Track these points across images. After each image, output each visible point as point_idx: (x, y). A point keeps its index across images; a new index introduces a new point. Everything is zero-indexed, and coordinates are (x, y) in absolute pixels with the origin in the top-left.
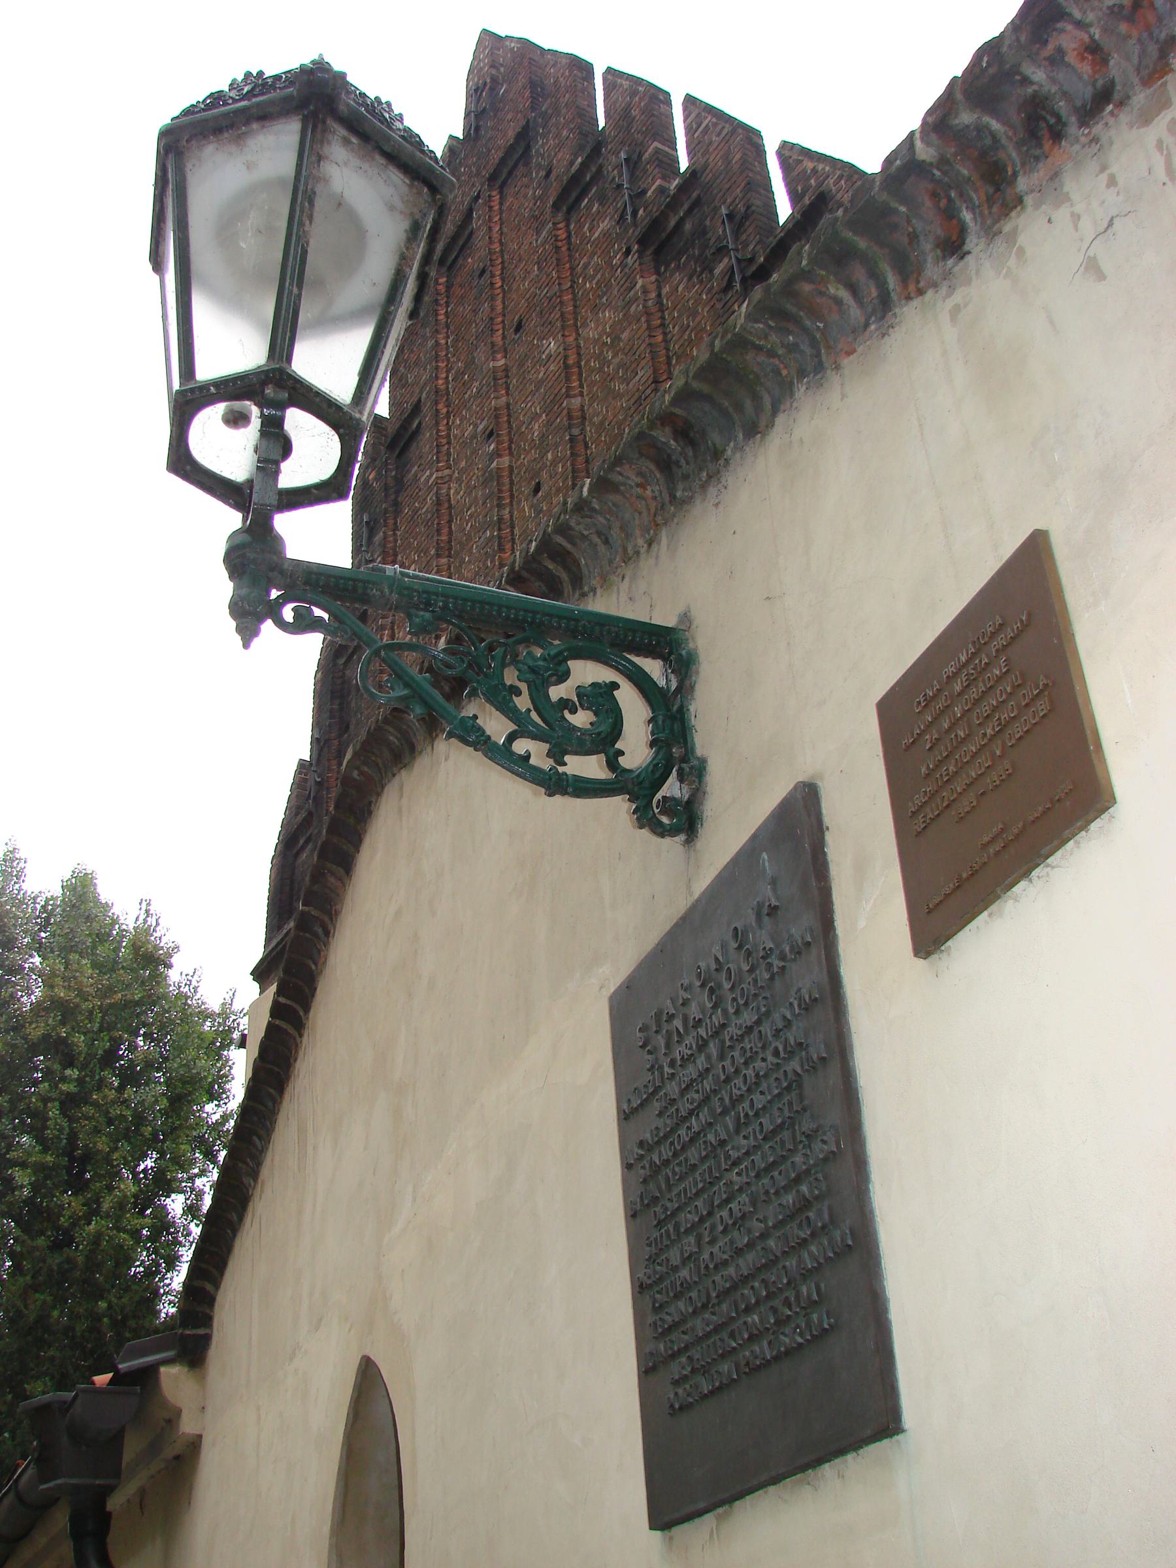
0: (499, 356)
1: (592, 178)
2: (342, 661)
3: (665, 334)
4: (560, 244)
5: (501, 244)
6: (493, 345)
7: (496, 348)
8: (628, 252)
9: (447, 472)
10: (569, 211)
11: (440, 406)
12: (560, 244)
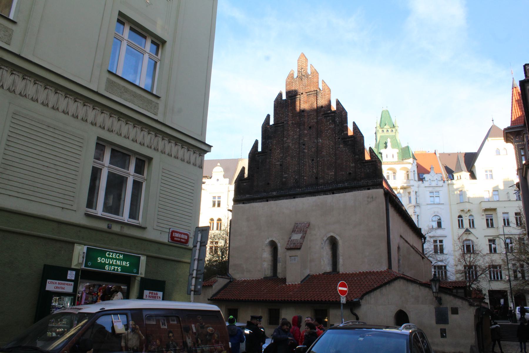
1: (331, 115)
2: (257, 155)
6: (305, 128)
8: (339, 138)
9: (290, 141)
10: (325, 117)
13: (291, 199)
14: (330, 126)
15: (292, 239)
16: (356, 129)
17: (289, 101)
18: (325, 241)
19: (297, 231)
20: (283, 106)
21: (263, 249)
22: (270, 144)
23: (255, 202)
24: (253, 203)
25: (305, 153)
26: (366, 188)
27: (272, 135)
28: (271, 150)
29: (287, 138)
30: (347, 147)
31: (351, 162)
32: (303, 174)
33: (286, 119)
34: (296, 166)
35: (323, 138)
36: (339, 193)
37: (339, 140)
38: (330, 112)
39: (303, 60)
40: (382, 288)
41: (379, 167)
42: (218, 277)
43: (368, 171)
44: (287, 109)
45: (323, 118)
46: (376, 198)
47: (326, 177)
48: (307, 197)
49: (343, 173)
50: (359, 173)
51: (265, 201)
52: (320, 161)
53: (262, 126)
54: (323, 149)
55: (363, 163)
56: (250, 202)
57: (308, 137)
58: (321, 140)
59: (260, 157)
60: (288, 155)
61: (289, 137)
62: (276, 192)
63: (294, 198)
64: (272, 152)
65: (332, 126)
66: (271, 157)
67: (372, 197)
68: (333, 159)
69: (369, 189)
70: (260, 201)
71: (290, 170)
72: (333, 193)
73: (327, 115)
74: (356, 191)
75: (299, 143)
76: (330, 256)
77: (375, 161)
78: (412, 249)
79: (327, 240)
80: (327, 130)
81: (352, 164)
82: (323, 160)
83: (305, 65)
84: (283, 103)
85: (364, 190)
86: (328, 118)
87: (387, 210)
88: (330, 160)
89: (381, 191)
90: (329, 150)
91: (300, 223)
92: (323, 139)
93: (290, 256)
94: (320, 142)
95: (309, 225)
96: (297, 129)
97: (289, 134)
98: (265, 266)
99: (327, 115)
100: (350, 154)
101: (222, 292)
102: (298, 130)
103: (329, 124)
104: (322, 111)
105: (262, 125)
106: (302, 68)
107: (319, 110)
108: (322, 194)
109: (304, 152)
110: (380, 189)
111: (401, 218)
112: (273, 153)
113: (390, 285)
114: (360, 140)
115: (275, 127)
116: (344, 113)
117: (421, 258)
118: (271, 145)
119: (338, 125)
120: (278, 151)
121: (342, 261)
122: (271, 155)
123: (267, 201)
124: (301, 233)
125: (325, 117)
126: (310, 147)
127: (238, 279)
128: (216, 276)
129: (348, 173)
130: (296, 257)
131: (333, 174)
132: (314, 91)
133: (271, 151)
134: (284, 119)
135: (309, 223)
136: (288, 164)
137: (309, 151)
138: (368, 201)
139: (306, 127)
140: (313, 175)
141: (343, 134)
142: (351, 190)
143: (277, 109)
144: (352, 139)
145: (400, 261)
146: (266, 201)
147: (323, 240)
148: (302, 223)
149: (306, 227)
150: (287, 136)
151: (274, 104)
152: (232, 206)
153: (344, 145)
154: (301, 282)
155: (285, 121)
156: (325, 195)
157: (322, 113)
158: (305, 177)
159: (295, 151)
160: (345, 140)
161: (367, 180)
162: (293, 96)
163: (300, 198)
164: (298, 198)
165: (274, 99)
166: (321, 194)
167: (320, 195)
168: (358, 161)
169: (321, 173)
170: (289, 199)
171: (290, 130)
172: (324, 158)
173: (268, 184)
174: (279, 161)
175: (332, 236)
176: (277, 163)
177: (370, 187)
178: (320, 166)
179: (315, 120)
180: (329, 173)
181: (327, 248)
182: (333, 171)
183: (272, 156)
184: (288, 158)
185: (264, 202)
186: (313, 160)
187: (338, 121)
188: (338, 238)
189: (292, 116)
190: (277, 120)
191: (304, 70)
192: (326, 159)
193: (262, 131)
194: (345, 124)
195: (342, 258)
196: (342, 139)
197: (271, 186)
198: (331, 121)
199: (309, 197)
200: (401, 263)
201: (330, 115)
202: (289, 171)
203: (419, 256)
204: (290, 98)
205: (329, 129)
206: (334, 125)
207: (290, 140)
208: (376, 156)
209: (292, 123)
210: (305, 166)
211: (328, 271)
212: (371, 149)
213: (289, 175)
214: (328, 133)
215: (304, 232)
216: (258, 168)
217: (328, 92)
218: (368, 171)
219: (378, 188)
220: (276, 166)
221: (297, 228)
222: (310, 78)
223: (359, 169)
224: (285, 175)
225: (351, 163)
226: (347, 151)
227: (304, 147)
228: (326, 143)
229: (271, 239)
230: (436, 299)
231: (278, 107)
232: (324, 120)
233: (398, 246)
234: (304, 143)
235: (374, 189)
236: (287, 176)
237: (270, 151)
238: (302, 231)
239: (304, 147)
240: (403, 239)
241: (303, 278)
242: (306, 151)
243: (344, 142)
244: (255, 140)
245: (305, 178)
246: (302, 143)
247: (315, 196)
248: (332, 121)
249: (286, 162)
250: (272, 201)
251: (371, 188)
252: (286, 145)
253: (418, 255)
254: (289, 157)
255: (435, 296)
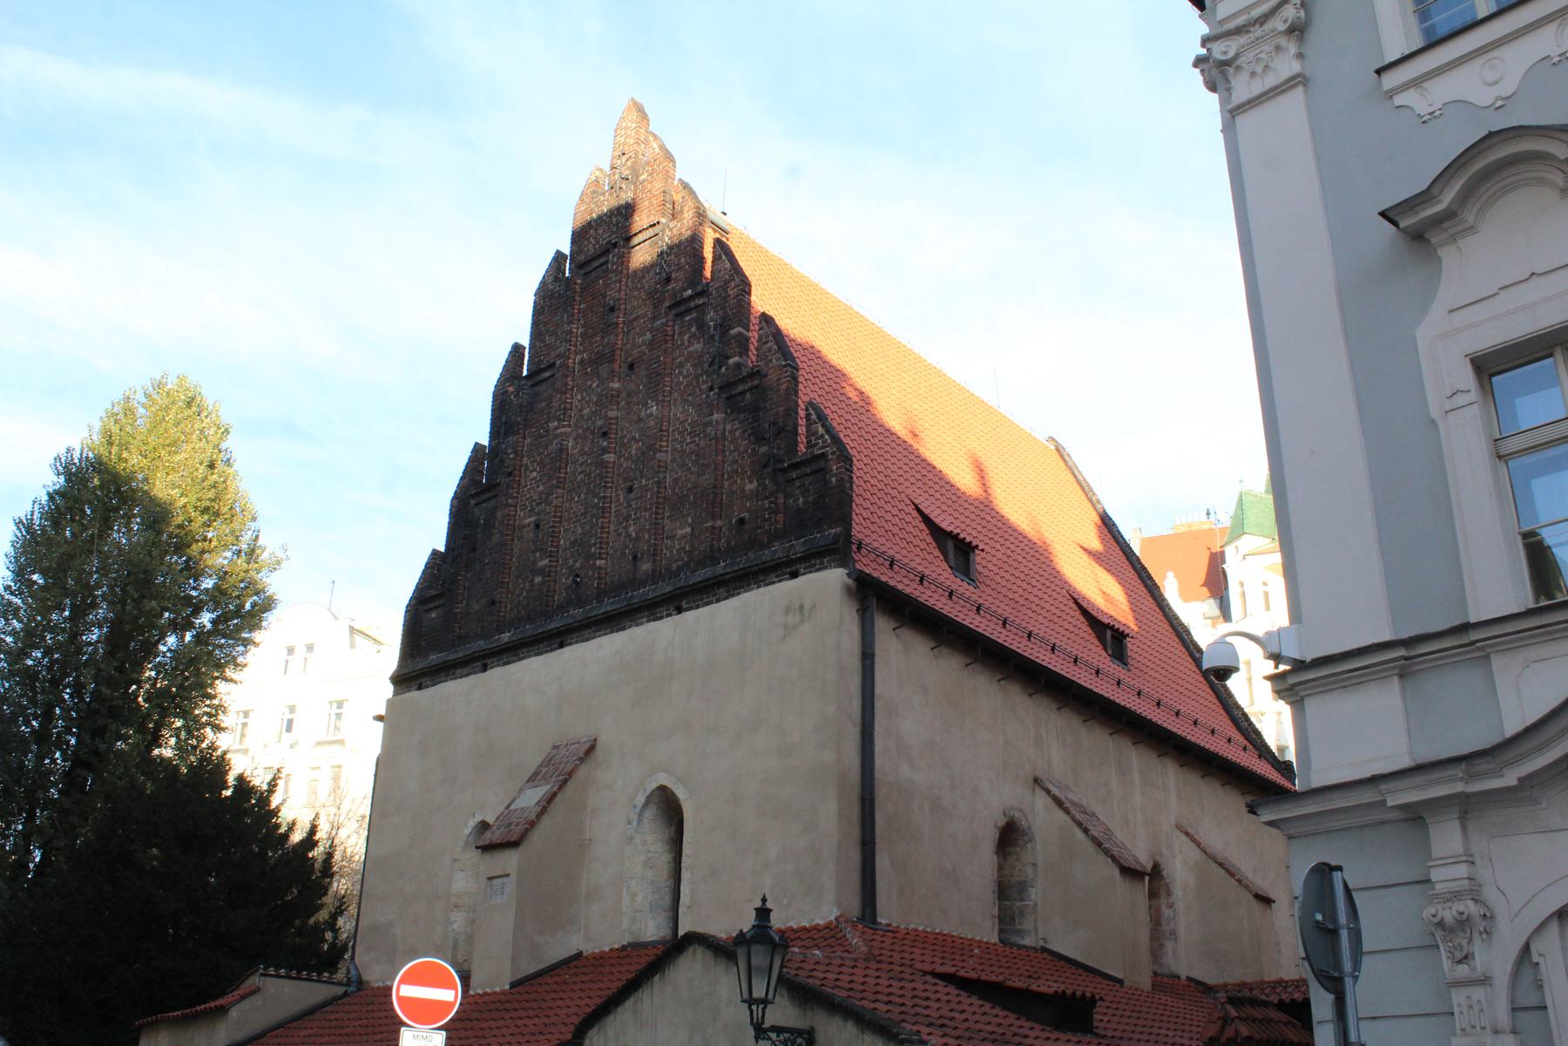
0: (616, 379)
2: (473, 502)
3: (724, 457)
4: (668, 338)
5: (626, 294)
6: (613, 371)
7: (615, 374)
8: (711, 389)
9: (569, 430)
11: (569, 379)
12: (668, 338)
13: (551, 651)
14: (691, 349)
15: (513, 807)
16: (767, 342)
17: (579, 281)
18: (638, 810)
19: (543, 776)
20: (559, 303)
21: (455, 860)
22: (510, 451)
23: (452, 679)
24: (446, 681)
25: (607, 467)
26: (786, 573)
27: (519, 419)
28: (510, 474)
29: (559, 420)
30: (738, 418)
31: (748, 478)
32: (593, 549)
33: (562, 350)
34: (579, 521)
35: (664, 396)
36: (698, 607)
37: (712, 393)
38: (690, 292)
39: (629, 125)
40: (640, 990)
41: (834, 480)
42: (262, 975)
43: (801, 500)
44: (567, 312)
45: (667, 321)
46: (814, 607)
47: (664, 551)
48: (600, 636)
49: (719, 523)
50: (767, 516)
51: (477, 670)
52: (648, 490)
53: (493, 389)
54: (661, 441)
55: (784, 470)
56: (437, 680)
57: (623, 403)
58: (655, 408)
59: (483, 505)
60: (558, 482)
61: (564, 414)
62: (512, 632)
63: (561, 646)
64: (513, 480)
65: (697, 346)
66: (510, 501)
67: (801, 607)
68: (692, 473)
69: (794, 575)
70: (465, 671)
71: (562, 542)
72: (679, 610)
73: (682, 308)
74: (753, 589)
75: (593, 433)
76: (666, 872)
77: (823, 455)
78: (1079, 834)
79: (646, 804)
80: (681, 365)
81: (751, 482)
82: (658, 482)
83: (632, 141)
84: (559, 295)
85: (779, 581)
86: (687, 318)
87: (867, 657)
88: (683, 478)
89: (833, 579)
90: (681, 442)
91: (566, 745)
92: (663, 401)
93: (490, 879)
94: (651, 414)
95: (591, 749)
96: (595, 379)
97: (567, 402)
98: (455, 926)
99: (682, 308)
100: (746, 442)
101: (268, 1035)
102: (594, 385)
103: (689, 342)
104: (667, 294)
105: (496, 386)
106: (624, 154)
107: (658, 294)
108: (645, 619)
109: (602, 464)
110: (831, 567)
111: (1054, 706)
112: (519, 485)
113: (664, 973)
114: (778, 380)
115: (532, 386)
116: (734, 288)
117: (1117, 872)
118: (512, 456)
119: (712, 337)
120: (535, 474)
121: (687, 892)
122: (511, 491)
123: (485, 668)
124: (548, 784)
125: (676, 316)
126: (625, 441)
127: (376, 985)
128: (257, 970)
129: (734, 521)
130: (505, 880)
131: (687, 533)
132: (651, 226)
133: (512, 478)
134: (558, 351)
135: (595, 740)
136: (555, 516)
137: (621, 457)
138: (785, 627)
139: (620, 367)
140: (627, 547)
141: (724, 369)
142: (735, 589)
143: (540, 318)
144: (756, 382)
145: (1032, 891)
146: (480, 672)
147: (635, 806)
148: (572, 744)
149: (575, 758)
150: (559, 413)
151: (535, 302)
152: (388, 701)
153: (729, 411)
154: (514, 985)
155: (559, 356)
156: (654, 620)
157: (667, 304)
158: (601, 558)
159: (581, 465)
160: (734, 392)
161: (790, 541)
162: (588, 262)
163: (576, 642)
164: (571, 644)
165: (535, 285)
166: (643, 617)
167: (637, 625)
168: (765, 466)
169: (646, 537)
170: (547, 652)
171: (572, 389)
172: (661, 476)
173: (493, 602)
174: (534, 509)
175: (663, 789)
176: (527, 521)
177: (798, 566)
178: (646, 510)
179: (648, 336)
180: (674, 532)
181: (650, 839)
182: (690, 520)
183: (512, 497)
184: (555, 496)
185: (475, 673)
186: (630, 490)
187: (712, 323)
188: (681, 793)
189: (583, 335)
190: (537, 360)
191: (627, 160)
192: (671, 476)
193: (492, 411)
194: (733, 328)
195: (689, 877)
196: (720, 388)
197: (500, 612)
198: (693, 329)
199: (606, 634)
200: (1033, 897)
201: (693, 304)
202: (558, 546)
203: (1110, 861)
204: (582, 272)
205: (687, 360)
206: (702, 340)
207: (569, 426)
208: (827, 437)
209: (582, 362)
210: (604, 517)
211: (651, 939)
212: (811, 411)
213: (558, 561)
214: (685, 377)
215: (561, 778)
216: (474, 550)
217: (692, 218)
218: (801, 500)
219: (826, 568)
220: (525, 530)
221: (547, 766)
222: (644, 181)
223: (767, 498)
224: (542, 559)
225: (747, 481)
226: (737, 433)
227: (605, 444)
228: (675, 415)
229: (481, 819)
230: (757, 1038)
231: (543, 314)
232: (674, 331)
233: (1002, 822)
234: (605, 430)
235: (811, 572)
236: (546, 566)
237: (507, 480)
238: (556, 774)
239: (605, 444)
240: (1043, 793)
241: (531, 968)
242: (610, 457)
243: (728, 398)
244: (472, 447)
245: (598, 562)
246: (601, 428)
247: (624, 629)
248: (698, 329)
249: (549, 513)
250: (498, 666)
251: (802, 570)
252: (553, 447)
253: (1103, 858)
254: (560, 491)
255: (755, 1021)
